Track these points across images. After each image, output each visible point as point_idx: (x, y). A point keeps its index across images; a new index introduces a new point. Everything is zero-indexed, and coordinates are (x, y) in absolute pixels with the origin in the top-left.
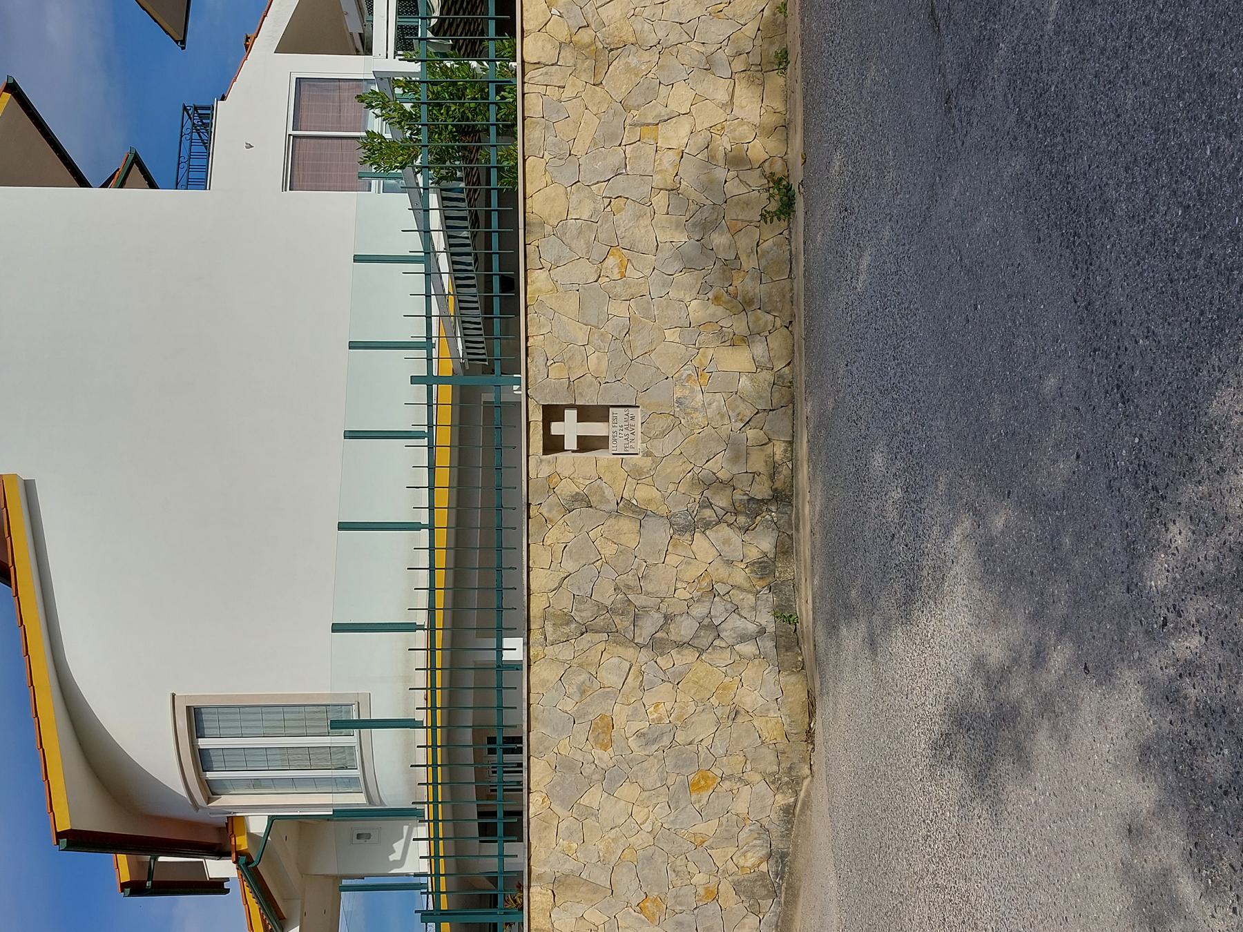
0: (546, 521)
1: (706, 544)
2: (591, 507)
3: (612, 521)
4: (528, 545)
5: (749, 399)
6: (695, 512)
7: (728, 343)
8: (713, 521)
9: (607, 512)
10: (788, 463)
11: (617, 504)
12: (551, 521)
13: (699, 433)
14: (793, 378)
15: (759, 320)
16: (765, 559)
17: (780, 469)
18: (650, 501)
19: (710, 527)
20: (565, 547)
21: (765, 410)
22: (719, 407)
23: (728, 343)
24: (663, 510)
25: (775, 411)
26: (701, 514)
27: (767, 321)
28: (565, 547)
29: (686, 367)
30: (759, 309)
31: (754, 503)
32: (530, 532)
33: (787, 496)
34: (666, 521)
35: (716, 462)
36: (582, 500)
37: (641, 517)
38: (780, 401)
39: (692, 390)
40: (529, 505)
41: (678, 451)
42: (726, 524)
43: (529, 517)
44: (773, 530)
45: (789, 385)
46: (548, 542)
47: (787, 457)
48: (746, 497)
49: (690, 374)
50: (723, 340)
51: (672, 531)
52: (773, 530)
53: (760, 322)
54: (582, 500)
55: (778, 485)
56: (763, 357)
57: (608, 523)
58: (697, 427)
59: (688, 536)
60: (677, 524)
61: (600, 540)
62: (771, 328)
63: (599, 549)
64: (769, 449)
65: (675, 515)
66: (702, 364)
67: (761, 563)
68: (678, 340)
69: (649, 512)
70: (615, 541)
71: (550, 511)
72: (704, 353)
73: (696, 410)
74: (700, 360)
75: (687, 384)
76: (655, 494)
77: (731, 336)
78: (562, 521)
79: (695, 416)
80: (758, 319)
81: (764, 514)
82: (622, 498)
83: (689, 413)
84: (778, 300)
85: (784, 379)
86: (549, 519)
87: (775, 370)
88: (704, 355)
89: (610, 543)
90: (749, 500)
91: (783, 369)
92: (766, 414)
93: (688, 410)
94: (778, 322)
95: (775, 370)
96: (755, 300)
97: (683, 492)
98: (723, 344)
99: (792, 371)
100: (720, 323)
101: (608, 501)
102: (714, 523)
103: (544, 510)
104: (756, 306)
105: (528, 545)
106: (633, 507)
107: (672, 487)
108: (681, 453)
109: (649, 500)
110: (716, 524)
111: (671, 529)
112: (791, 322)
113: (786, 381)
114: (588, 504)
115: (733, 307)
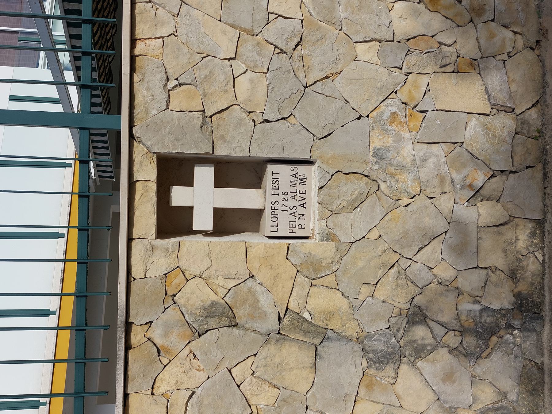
0: (159, 352)
1: (416, 382)
2: (236, 325)
3: (270, 350)
4: (126, 396)
5: (480, 154)
6: (402, 332)
7: (450, 69)
8: (429, 345)
9: (263, 335)
10: (536, 253)
11: (279, 319)
12: (168, 352)
13: (407, 206)
14: (543, 125)
15: (493, 37)
16: (505, 404)
17: (525, 263)
18: (330, 314)
19: (423, 355)
20: (191, 396)
21: (502, 171)
22: (437, 165)
23: (450, 69)
24: (351, 329)
25: (517, 174)
26: (410, 334)
27: (504, 39)
28: (191, 396)
29: (388, 101)
30: (493, 20)
31: (488, 316)
32: (130, 373)
33: (535, 305)
34: (357, 347)
35: (434, 252)
36: (222, 315)
37: (317, 341)
38: (525, 159)
39: (398, 139)
40: (128, 325)
41: (374, 234)
42: (446, 349)
43: (128, 347)
44: (517, 357)
45: (537, 134)
46: (161, 388)
47: (536, 245)
48: (477, 307)
49: (394, 113)
50: (444, 62)
51: (365, 364)
52: (517, 357)
53: (495, 40)
54: (222, 315)
55: (522, 287)
56: (501, 91)
57: (263, 353)
58: (405, 195)
59: (389, 370)
60: (374, 352)
61: (251, 382)
62: (511, 49)
63: (248, 397)
64: (508, 233)
65: (369, 337)
66: (412, 98)
67: (497, 409)
68: (375, 59)
69: (330, 333)
70: (275, 383)
71: (166, 335)
72: (415, 81)
73: (402, 168)
74: (410, 91)
75: (390, 128)
76: (341, 303)
77: (454, 57)
78: (186, 351)
79: (401, 178)
80: (492, 36)
81: (502, 332)
82: (287, 309)
83: (392, 174)
84: (520, 9)
85: (530, 126)
86: (164, 348)
87: (518, 111)
88: (416, 86)
89: (266, 386)
90: (482, 311)
91: (529, 112)
92: (504, 178)
93: (392, 169)
94: (520, 42)
95: (518, 111)
96: (487, 7)
97: (382, 298)
98: (443, 69)
99: (543, 114)
100: (439, 38)
101: (264, 316)
102: (429, 348)
103: (156, 334)
104: (488, 16)
105: (126, 396)
106: (305, 325)
107: (365, 291)
108: (380, 236)
109: (330, 312)
110: (433, 350)
111: (364, 360)
112: (538, 42)
113: (532, 128)
114: (231, 321)
115: (456, 16)
